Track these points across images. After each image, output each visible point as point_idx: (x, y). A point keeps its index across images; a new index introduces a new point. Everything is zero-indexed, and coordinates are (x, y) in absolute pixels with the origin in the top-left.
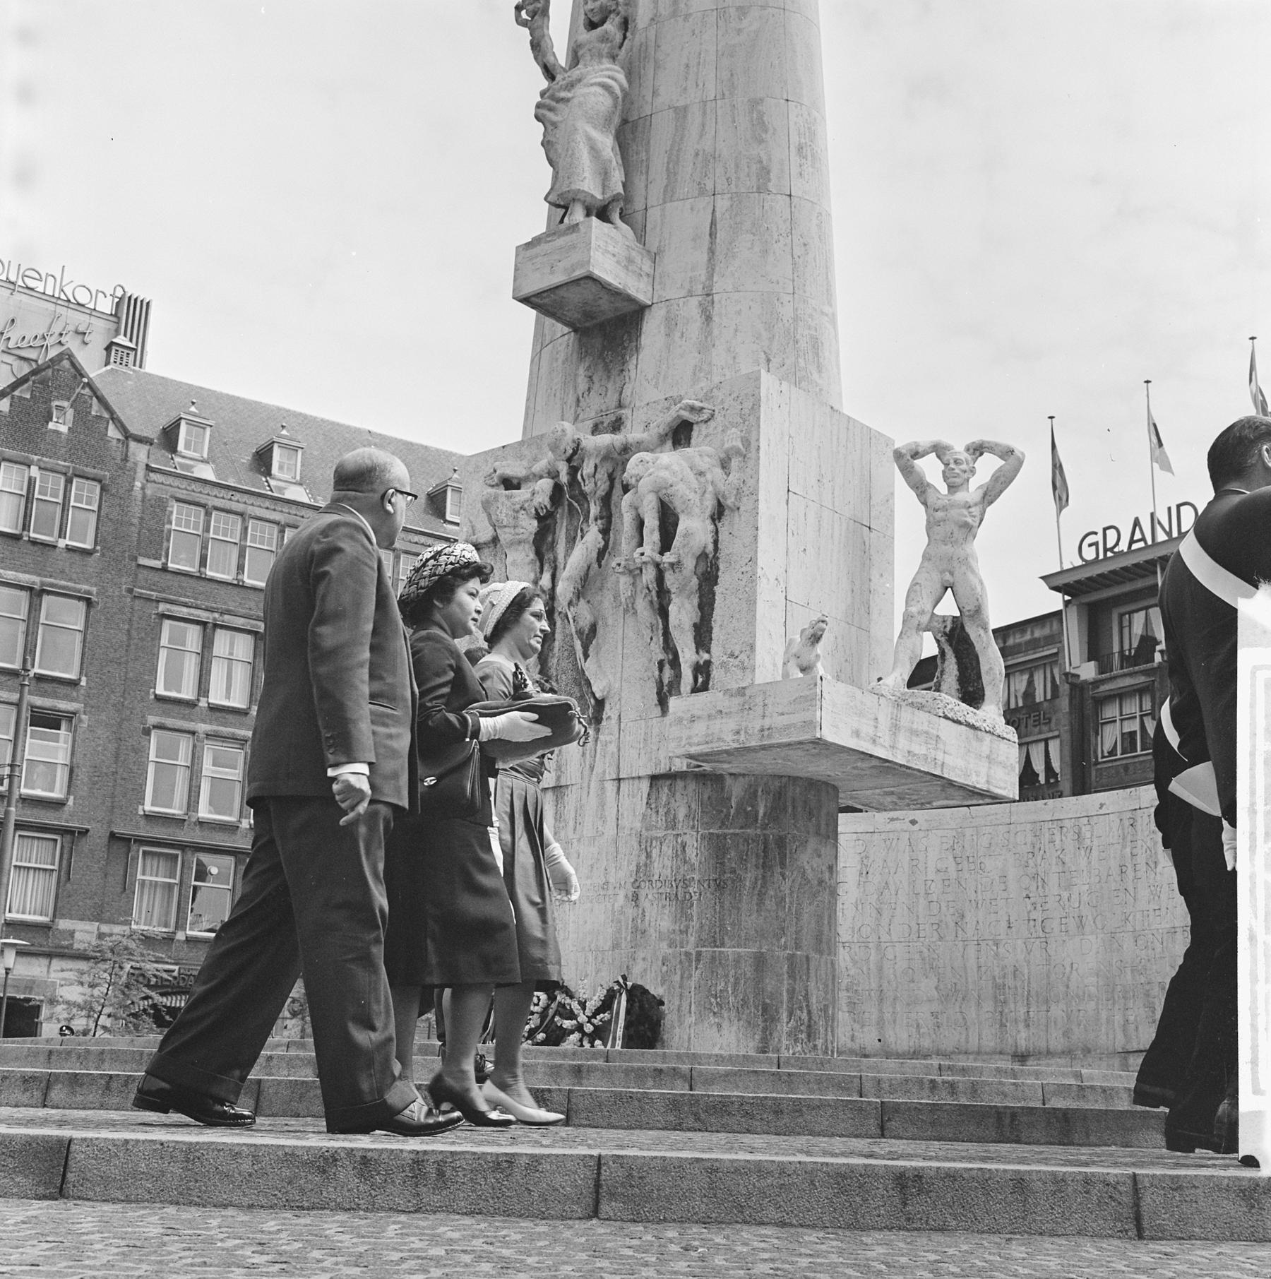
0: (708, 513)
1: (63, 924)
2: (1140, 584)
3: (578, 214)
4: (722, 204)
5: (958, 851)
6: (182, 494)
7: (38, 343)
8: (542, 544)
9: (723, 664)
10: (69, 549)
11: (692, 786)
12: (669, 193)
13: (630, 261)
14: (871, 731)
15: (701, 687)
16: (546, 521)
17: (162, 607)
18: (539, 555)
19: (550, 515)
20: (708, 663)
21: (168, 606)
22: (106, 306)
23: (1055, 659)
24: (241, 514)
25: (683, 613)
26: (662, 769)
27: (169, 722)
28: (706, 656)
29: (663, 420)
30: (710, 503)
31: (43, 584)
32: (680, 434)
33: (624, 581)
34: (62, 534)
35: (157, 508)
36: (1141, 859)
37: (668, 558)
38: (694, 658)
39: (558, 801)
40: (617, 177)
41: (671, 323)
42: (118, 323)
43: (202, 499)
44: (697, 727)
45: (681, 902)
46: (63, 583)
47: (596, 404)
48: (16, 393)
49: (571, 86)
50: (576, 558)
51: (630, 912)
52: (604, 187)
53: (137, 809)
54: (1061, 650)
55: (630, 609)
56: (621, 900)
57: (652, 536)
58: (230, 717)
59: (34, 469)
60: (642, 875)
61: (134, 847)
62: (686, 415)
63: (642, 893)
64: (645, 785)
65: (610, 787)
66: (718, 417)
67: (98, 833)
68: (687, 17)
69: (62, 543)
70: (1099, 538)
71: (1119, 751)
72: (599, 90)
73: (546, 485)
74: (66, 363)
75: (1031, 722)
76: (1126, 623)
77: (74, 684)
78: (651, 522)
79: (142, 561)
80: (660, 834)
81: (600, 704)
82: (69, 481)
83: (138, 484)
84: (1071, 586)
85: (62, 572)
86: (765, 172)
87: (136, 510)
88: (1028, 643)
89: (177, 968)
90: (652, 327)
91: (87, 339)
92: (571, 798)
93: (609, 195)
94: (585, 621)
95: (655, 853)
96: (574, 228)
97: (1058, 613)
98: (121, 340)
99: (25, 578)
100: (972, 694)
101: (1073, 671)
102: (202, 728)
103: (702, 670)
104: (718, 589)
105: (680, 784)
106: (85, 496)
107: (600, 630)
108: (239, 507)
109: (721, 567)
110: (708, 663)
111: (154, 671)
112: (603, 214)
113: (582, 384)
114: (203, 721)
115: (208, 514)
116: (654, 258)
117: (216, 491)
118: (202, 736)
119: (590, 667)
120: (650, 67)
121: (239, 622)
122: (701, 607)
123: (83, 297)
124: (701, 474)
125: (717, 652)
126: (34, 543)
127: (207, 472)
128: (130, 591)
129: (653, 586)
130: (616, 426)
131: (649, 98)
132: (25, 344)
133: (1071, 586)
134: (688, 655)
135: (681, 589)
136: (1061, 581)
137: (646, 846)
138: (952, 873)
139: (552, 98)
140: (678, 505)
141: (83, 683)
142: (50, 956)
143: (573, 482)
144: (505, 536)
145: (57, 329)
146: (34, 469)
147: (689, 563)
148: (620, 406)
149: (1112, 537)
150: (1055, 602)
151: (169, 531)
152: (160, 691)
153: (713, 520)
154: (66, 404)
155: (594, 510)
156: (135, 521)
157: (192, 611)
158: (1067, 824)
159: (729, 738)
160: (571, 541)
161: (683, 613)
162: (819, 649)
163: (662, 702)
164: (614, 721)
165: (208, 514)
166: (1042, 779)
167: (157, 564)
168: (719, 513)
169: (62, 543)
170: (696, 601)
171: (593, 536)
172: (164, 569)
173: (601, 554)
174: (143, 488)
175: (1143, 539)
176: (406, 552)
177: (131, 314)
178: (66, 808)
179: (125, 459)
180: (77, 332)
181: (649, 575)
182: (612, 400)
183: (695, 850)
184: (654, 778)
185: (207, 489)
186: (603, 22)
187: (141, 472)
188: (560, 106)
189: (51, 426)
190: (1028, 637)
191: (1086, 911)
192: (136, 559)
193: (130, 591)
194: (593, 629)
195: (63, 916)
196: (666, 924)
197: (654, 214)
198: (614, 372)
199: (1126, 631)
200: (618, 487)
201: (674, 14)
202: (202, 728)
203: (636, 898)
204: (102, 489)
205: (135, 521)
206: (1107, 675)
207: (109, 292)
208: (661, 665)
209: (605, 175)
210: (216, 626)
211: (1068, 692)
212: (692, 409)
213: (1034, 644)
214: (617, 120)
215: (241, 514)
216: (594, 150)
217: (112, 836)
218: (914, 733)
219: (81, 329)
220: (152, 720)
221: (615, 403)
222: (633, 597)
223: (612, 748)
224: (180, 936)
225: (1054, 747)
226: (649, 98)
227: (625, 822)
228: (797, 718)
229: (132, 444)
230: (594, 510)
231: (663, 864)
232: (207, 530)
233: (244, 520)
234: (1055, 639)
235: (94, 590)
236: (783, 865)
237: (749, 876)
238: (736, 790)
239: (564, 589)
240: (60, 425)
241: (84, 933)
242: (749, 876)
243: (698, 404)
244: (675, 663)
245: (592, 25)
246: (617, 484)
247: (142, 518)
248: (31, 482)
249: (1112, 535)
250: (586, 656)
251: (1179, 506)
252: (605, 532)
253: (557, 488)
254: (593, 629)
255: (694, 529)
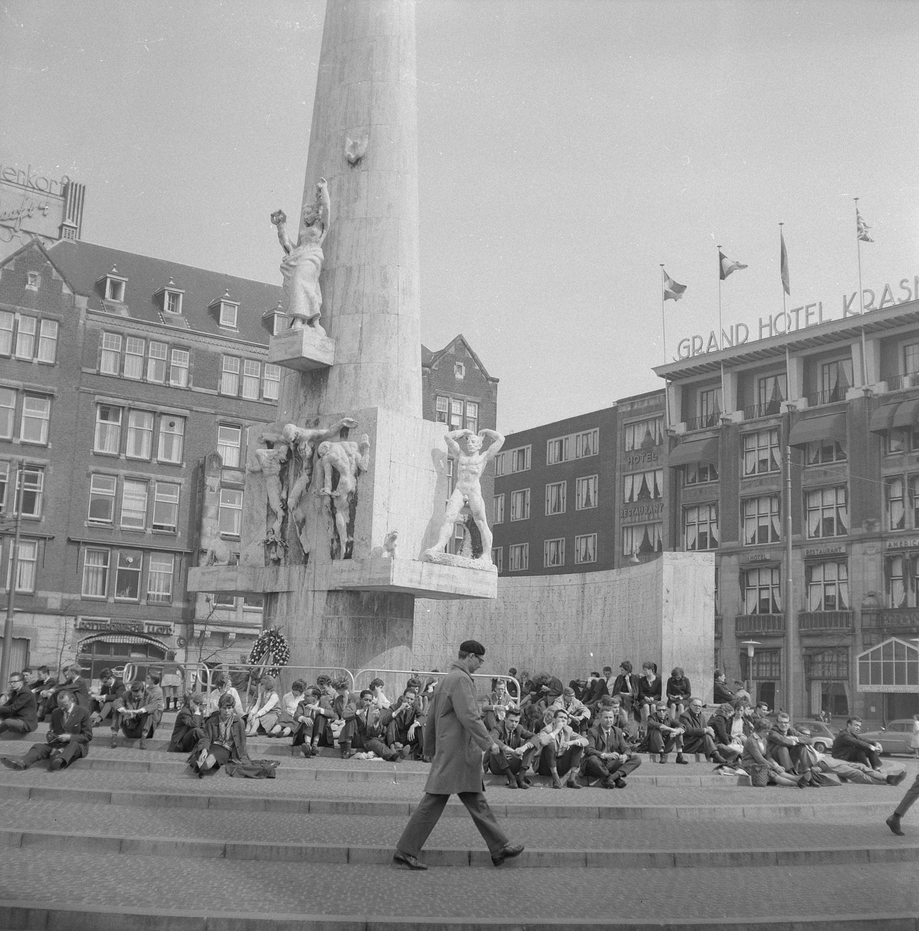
0: (354, 472)
1: (41, 594)
2: (712, 375)
3: (299, 325)
4: (366, 318)
5: (506, 599)
6: (108, 327)
7: (16, 216)
8: (283, 476)
9: (359, 543)
10: (41, 364)
11: (346, 595)
12: (342, 311)
13: (323, 346)
14: (418, 578)
15: (348, 556)
16: (284, 465)
17: (97, 398)
18: (282, 480)
19: (286, 463)
20: (352, 542)
21: (101, 397)
22: (57, 190)
23: (661, 418)
24: (145, 338)
25: (342, 519)
26: (332, 589)
27: (102, 469)
28: (351, 539)
29: (335, 426)
30: (354, 468)
31: (24, 386)
32: (344, 432)
33: (317, 501)
34: (35, 354)
35: (94, 337)
36: (586, 608)
37: (335, 493)
38: (346, 540)
39: (288, 598)
40: (318, 300)
41: (342, 375)
42: (65, 201)
43: (121, 329)
44: (346, 574)
45: (339, 647)
46: (36, 385)
47: (309, 411)
48: (5, 267)
49: (296, 259)
50: (298, 486)
51: (317, 651)
52: (311, 310)
53: (83, 523)
54: (664, 414)
55: (320, 513)
56: (314, 645)
57: (329, 483)
58: (139, 465)
59: (17, 314)
60: (323, 635)
61: (82, 548)
62: (345, 424)
63: (323, 644)
64: (325, 594)
65: (310, 594)
66: (360, 427)
67: (61, 540)
68: (353, 220)
69: (35, 361)
70: (690, 343)
71: (697, 480)
72: (311, 263)
73: (284, 448)
74: (36, 247)
75: (646, 459)
76: (705, 398)
77: (44, 447)
78: (328, 477)
79: (85, 370)
80: (331, 617)
81: (307, 555)
82: (39, 322)
83: (81, 322)
84: (672, 375)
85: (36, 378)
86: (386, 303)
87: (80, 337)
88: (646, 408)
89: (109, 619)
90: (333, 376)
91: (46, 212)
92: (294, 597)
93: (313, 314)
94: (300, 516)
95: (329, 626)
96: (295, 333)
97: (663, 391)
98: (68, 222)
99: (14, 383)
100: (477, 551)
101: (672, 428)
102: (123, 472)
103: (350, 545)
104: (357, 508)
105: (340, 594)
106: (49, 331)
107: (308, 521)
108: (144, 334)
109: (359, 498)
110: (352, 542)
111: (92, 438)
112: (310, 322)
113: (302, 400)
114: (123, 469)
115: (124, 339)
116: (337, 339)
117: (129, 324)
118: (122, 477)
119: (302, 539)
120: (336, 243)
121: (144, 406)
122: (350, 515)
123: (43, 185)
124: (350, 455)
125: (356, 538)
126: (19, 360)
127: (124, 313)
128: (78, 389)
129: (329, 505)
130: (317, 423)
131: (335, 260)
132: (6, 217)
133: (672, 375)
134: (344, 539)
135: (341, 507)
136: (664, 372)
137: (326, 622)
138: (503, 611)
139: (287, 264)
140: (339, 469)
141: (50, 447)
142: (34, 612)
143: (296, 450)
144: (266, 472)
145: (26, 207)
146: (17, 314)
147: (345, 497)
148: (319, 414)
149: (698, 343)
150: (662, 384)
151: (101, 351)
152: (97, 449)
153: (356, 476)
154: (36, 273)
155: (305, 464)
156: (80, 345)
157: (116, 400)
158: (555, 588)
159: (356, 581)
160: (296, 476)
161: (342, 519)
162: (396, 542)
163: (333, 557)
164: (313, 564)
165: (124, 339)
166: (652, 496)
167: (94, 371)
168: (358, 472)
169: (35, 361)
170: (348, 513)
171: (304, 478)
172: (98, 374)
173: (308, 485)
174: (84, 324)
175: (716, 345)
176: (247, 358)
177: (72, 195)
178: (41, 524)
179: (74, 307)
180: (40, 209)
181: (327, 501)
182: (315, 408)
183: (347, 626)
184: (329, 591)
185: (124, 323)
186: (313, 224)
187: (83, 313)
188: (291, 268)
189: (27, 287)
190: (646, 404)
191: (561, 633)
192: (81, 369)
193: (78, 389)
194: (304, 521)
195: (40, 589)
196: (333, 657)
197: (335, 319)
198: (316, 397)
199: (705, 402)
200: (316, 455)
201: (347, 218)
202: (123, 472)
203: (320, 645)
204: (60, 326)
205: (80, 345)
206: (691, 432)
207: (59, 181)
208: (332, 541)
209: (311, 304)
210: (130, 409)
211: (668, 442)
212: (348, 422)
213: (650, 409)
214: (318, 274)
215: (145, 338)
216: (307, 293)
217: (69, 540)
218: (440, 576)
219: (42, 206)
220: (92, 468)
221: (315, 412)
222: (321, 508)
223: (312, 576)
224: (111, 600)
225: (660, 477)
226: (335, 260)
227: (316, 611)
228: (382, 576)
229: (77, 297)
230: (305, 464)
231: (333, 630)
232: (124, 349)
233: (146, 342)
234: (661, 407)
235: (56, 389)
236: (385, 632)
237: (370, 637)
238: (365, 597)
239: (291, 502)
240: (33, 287)
241: (54, 600)
242: (370, 637)
243: (351, 420)
244: (338, 540)
245: (308, 225)
246: (316, 455)
247: (84, 343)
248: (16, 323)
249: (698, 341)
250: (301, 533)
251: (737, 326)
252: (310, 475)
253: (289, 450)
254: (304, 521)
255: (348, 481)
